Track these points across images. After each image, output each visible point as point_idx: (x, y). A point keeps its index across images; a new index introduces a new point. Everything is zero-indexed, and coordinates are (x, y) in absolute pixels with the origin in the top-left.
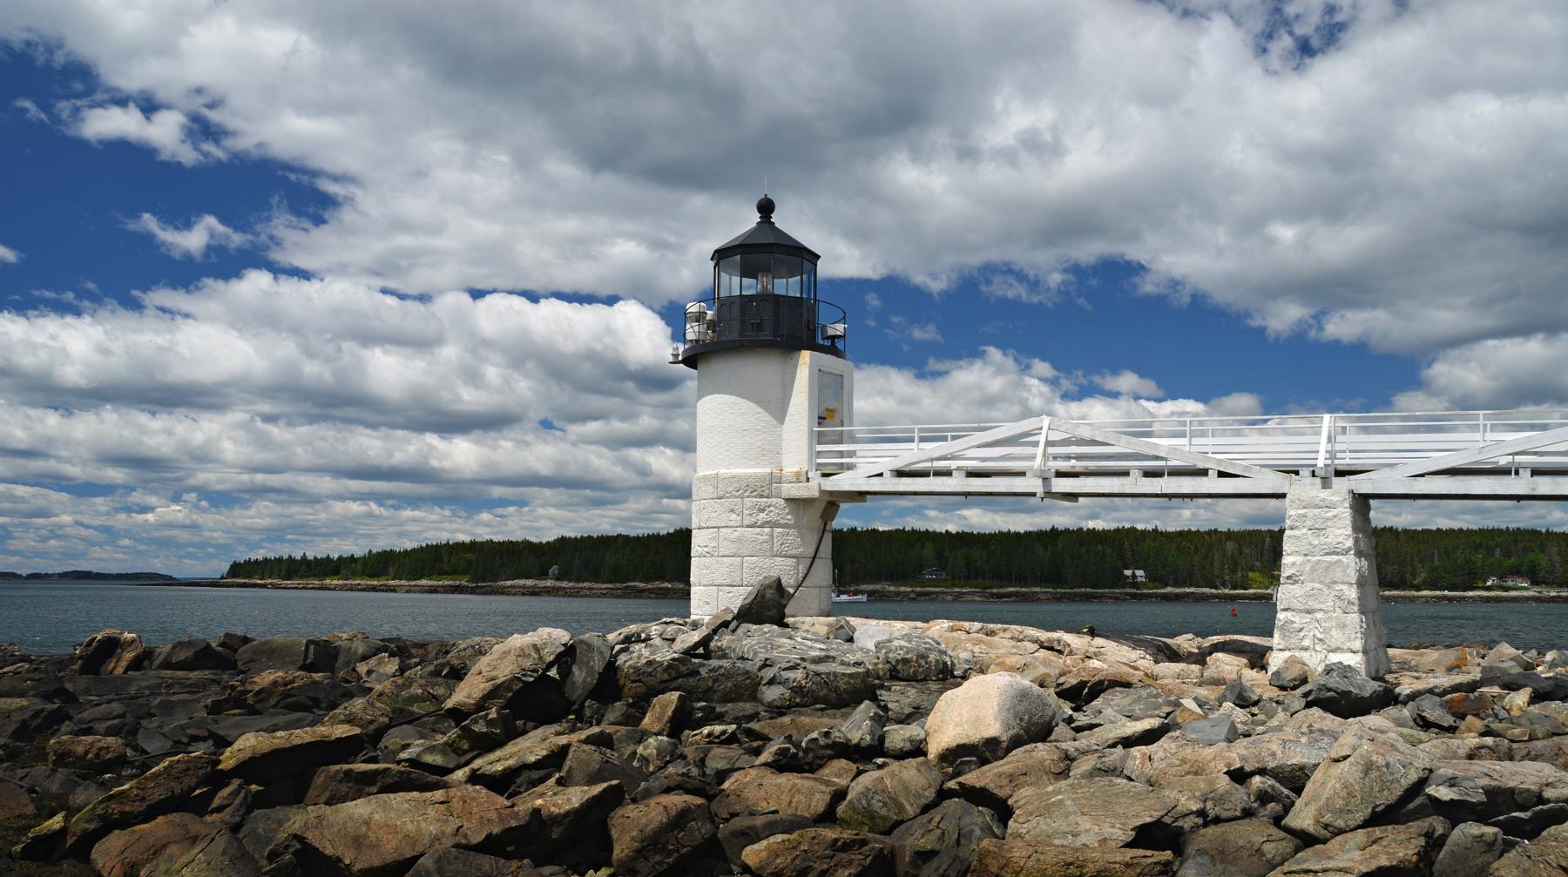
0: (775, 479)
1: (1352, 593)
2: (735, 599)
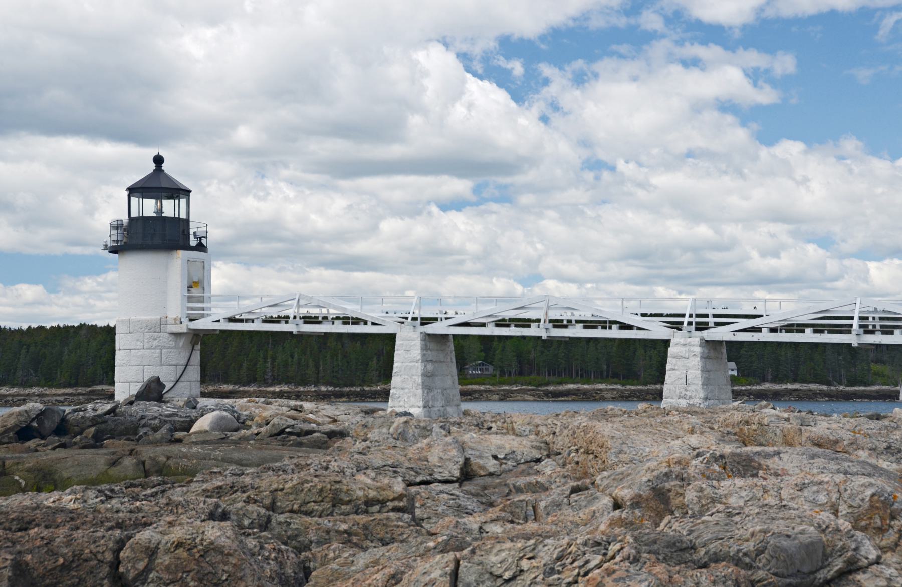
1: (419, 380)
2: (135, 389)
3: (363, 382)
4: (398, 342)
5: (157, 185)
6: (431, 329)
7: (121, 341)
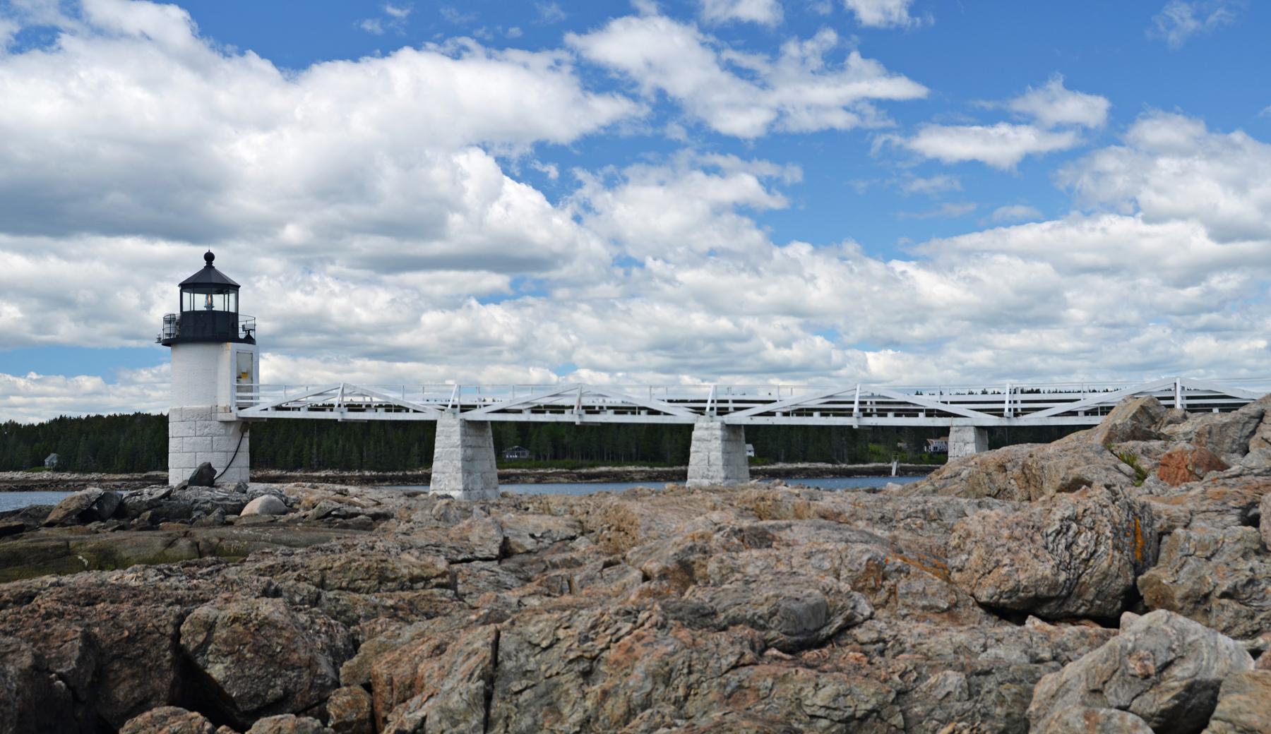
0: (214, 410)
1: (459, 465)
2: (188, 474)
3: (406, 468)
4: (438, 429)
5: (208, 280)
6: (470, 416)
7: (173, 429)
